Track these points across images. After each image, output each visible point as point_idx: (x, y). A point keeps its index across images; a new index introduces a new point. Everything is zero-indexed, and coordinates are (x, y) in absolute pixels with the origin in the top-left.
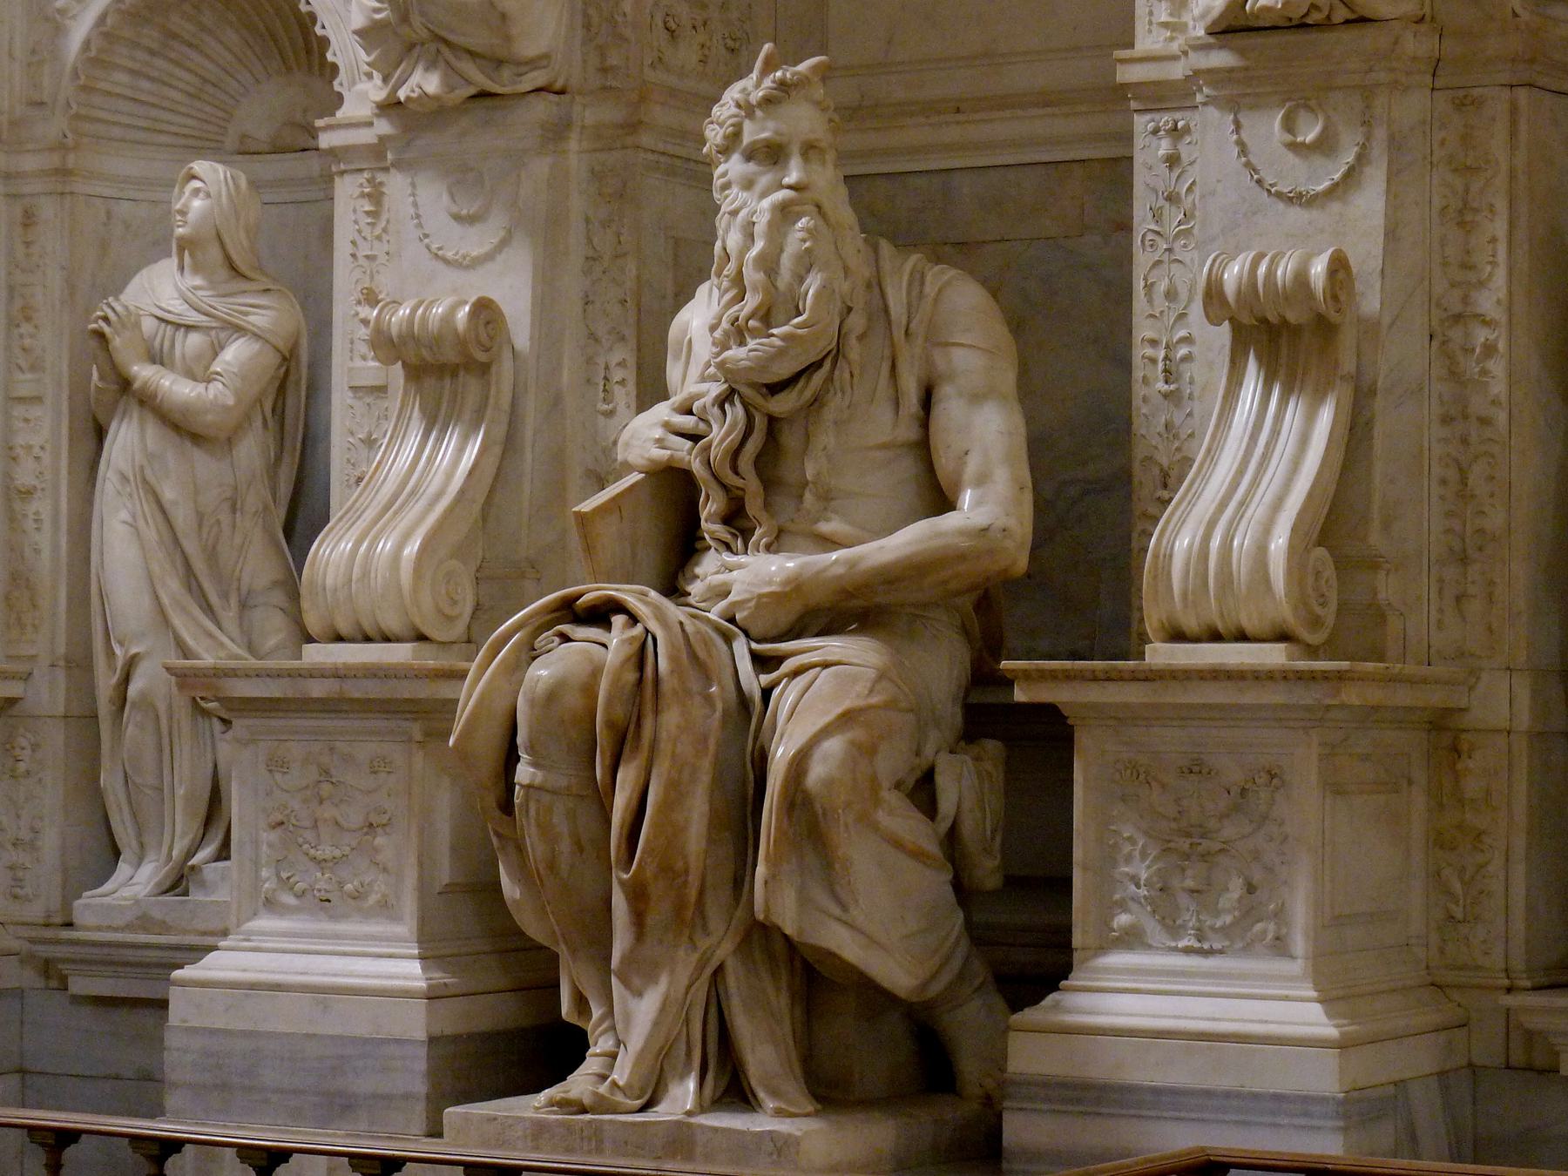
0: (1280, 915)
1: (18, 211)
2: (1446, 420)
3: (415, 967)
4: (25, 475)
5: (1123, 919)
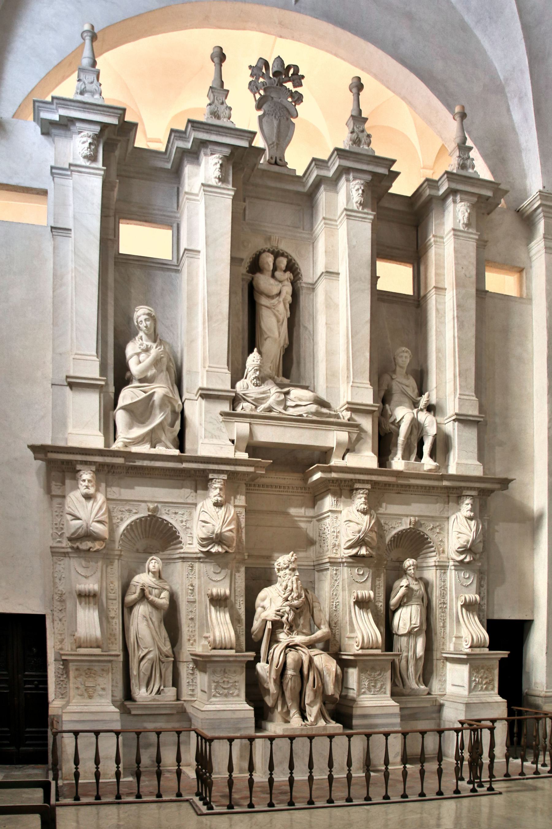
0: (385, 688)
5: (363, 690)
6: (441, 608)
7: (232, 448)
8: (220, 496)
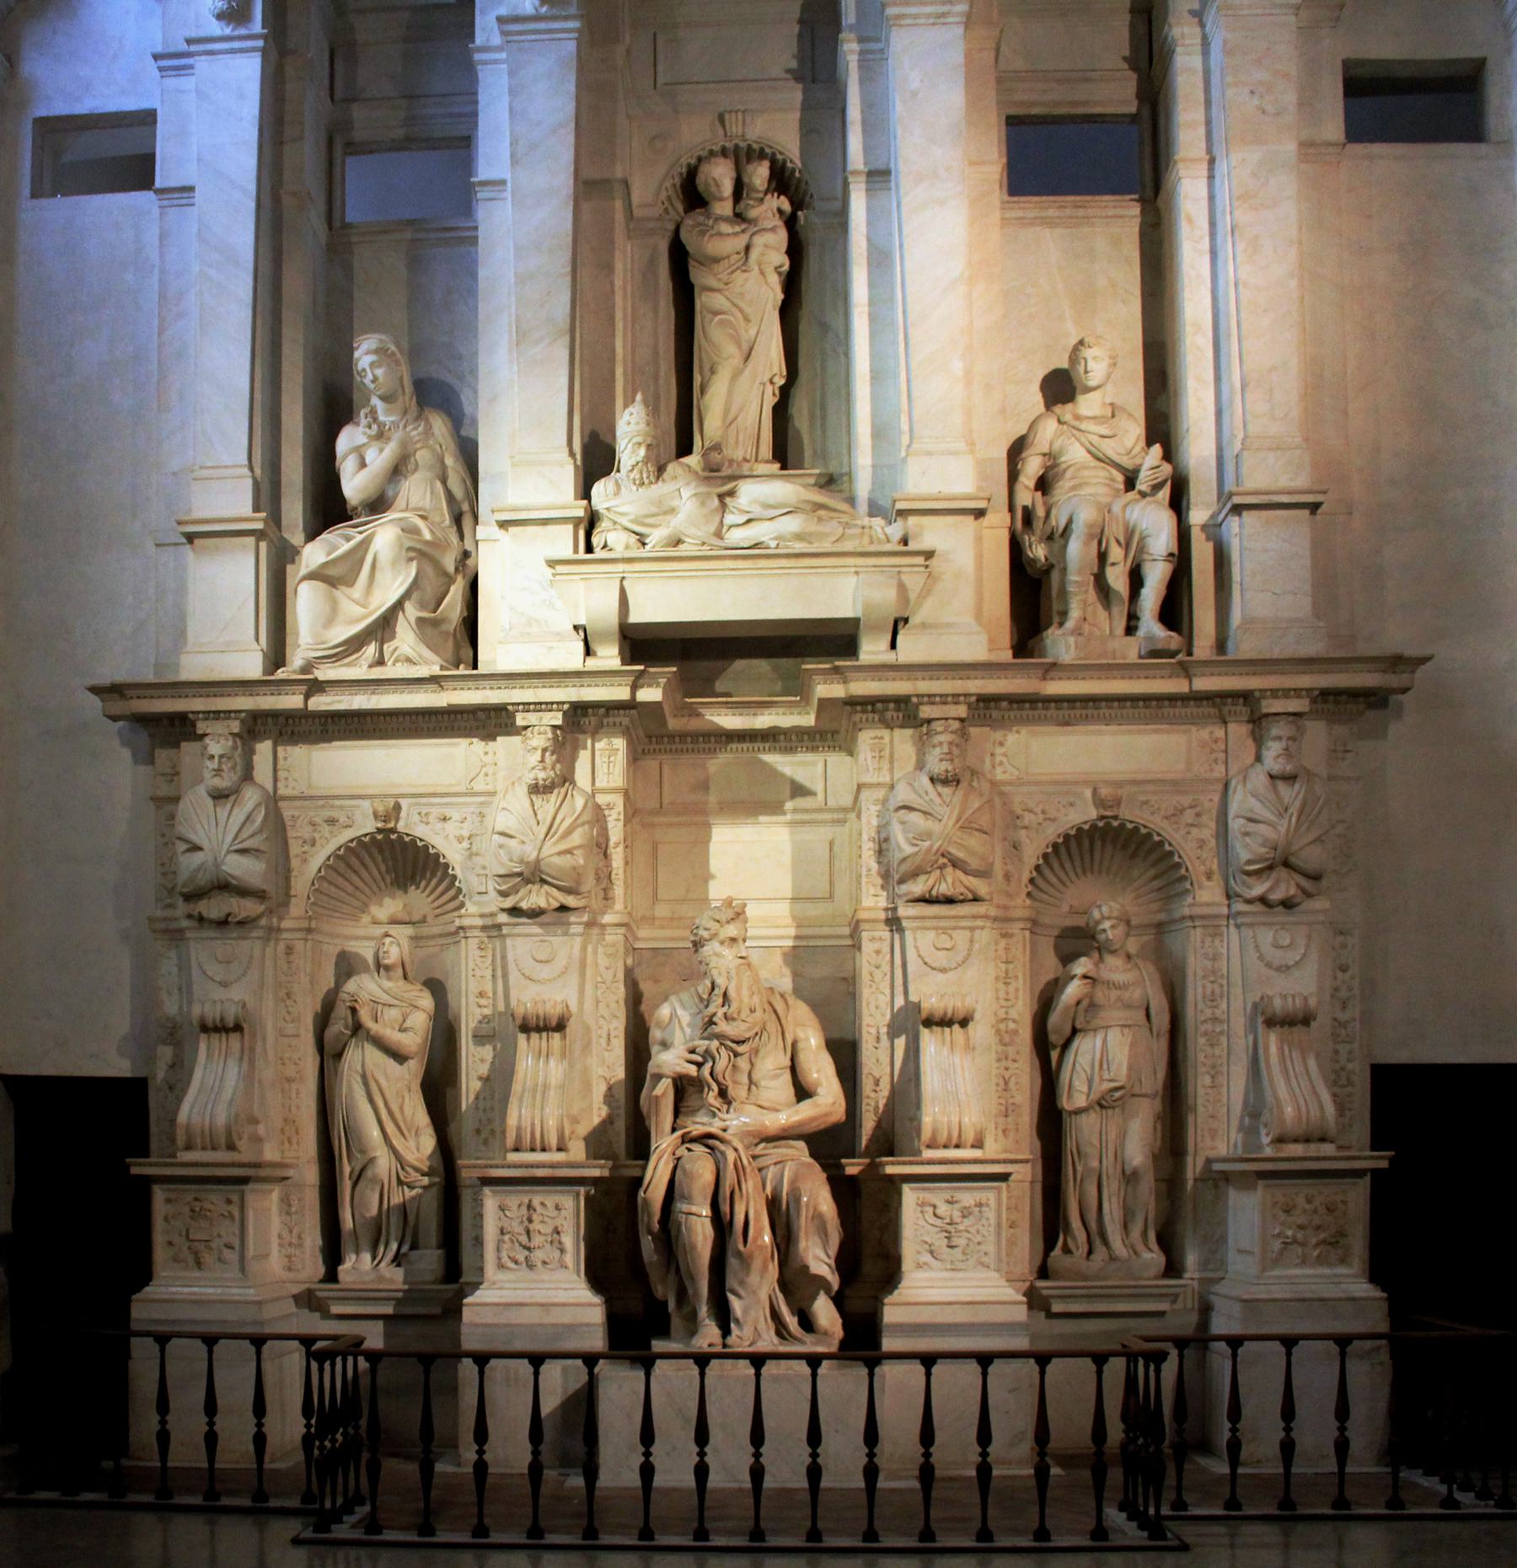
1: (282, 947)
2: (999, 1060)
4: (290, 1071)
6: (1205, 1033)
8: (544, 768)
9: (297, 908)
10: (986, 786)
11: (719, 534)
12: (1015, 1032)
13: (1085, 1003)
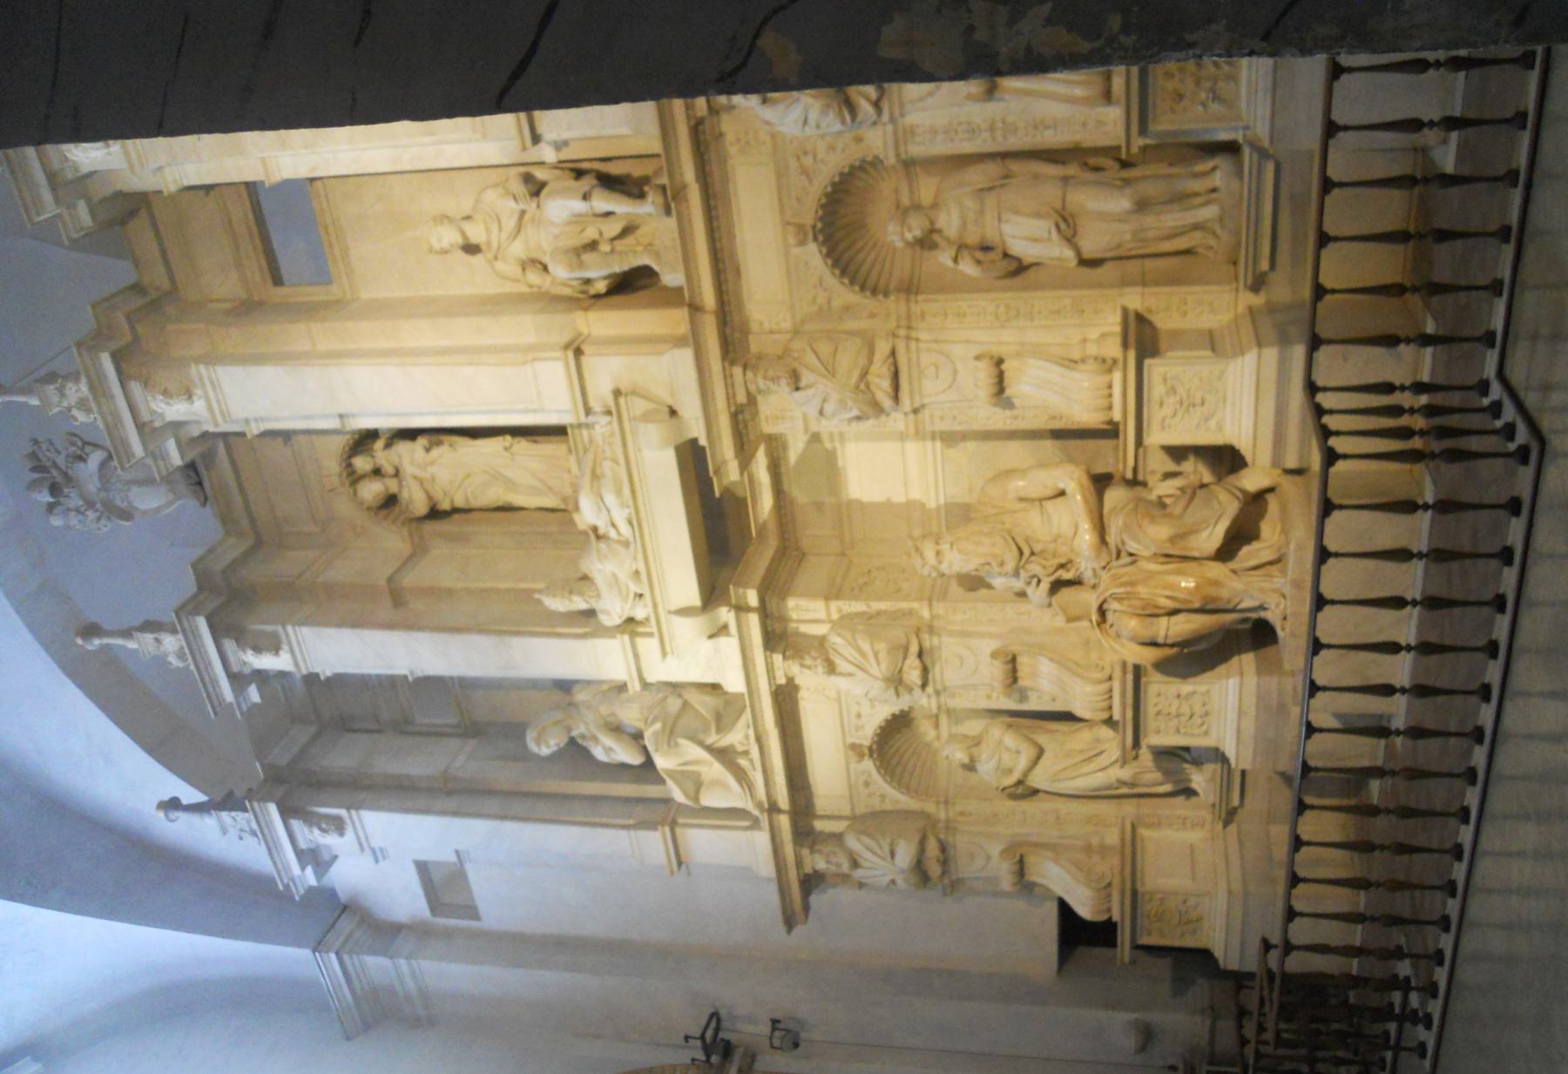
1: (960, 819)
3: (1231, 681)
6: (1005, 137)
7: (723, 640)
9: (930, 808)
10: (797, 345)
11: (626, 544)
12: (1007, 306)
13: (979, 255)
